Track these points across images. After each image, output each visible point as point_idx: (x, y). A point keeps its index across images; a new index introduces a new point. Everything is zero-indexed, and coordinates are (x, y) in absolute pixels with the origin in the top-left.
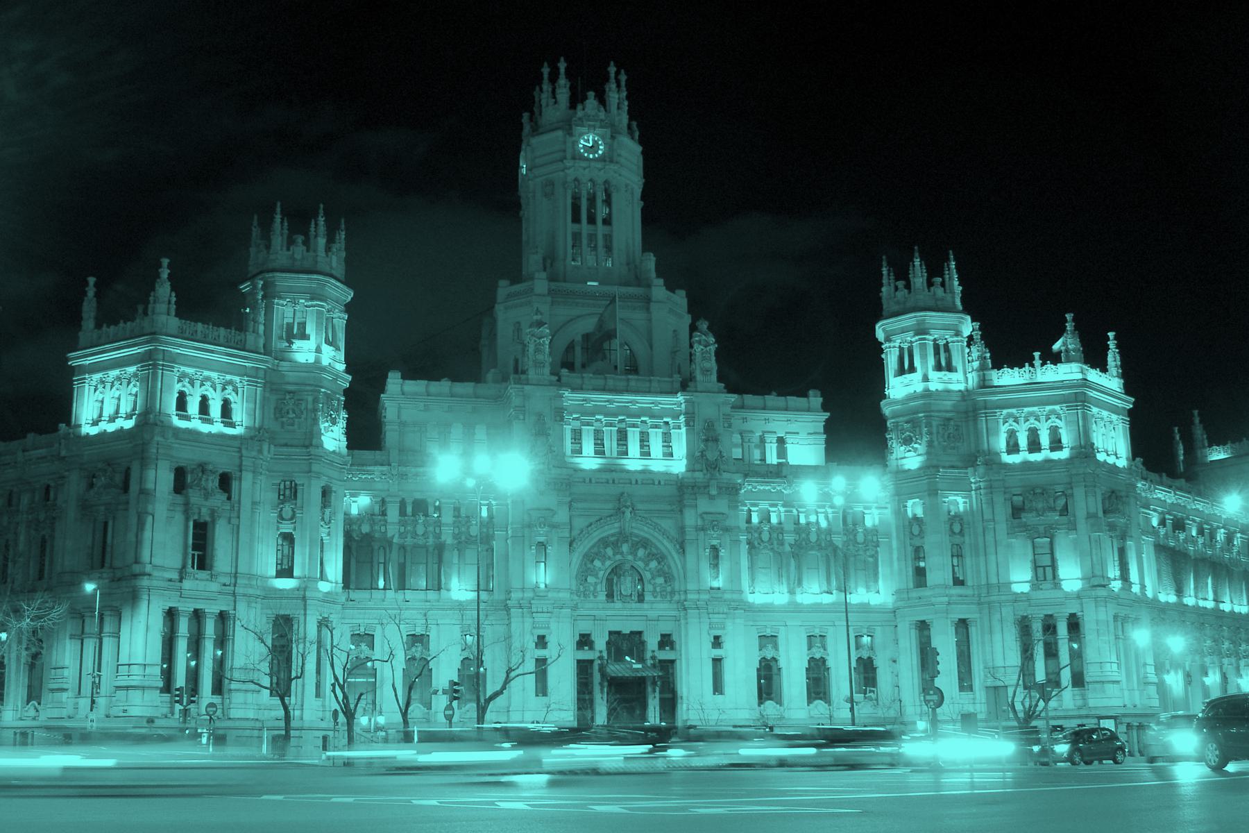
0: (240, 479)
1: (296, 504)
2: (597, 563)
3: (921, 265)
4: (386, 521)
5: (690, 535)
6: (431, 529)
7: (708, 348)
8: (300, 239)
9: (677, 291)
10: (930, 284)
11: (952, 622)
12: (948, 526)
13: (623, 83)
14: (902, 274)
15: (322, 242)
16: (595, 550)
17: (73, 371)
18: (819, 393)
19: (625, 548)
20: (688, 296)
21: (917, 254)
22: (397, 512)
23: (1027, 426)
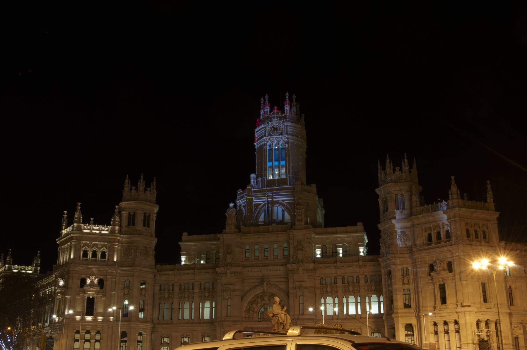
0: (106, 281)
1: (129, 289)
2: (254, 306)
3: (390, 163)
4: (174, 293)
5: (291, 291)
6: (190, 295)
7: (300, 211)
8: (133, 188)
9: (312, 185)
10: (394, 170)
11: (403, 325)
12: (401, 281)
13: (294, 99)
14: (384, 168)
15: (141, 188)
16: (253, 300)
17: (58, 245)
18: (361, 224)
19: (266, 299)
20: (317, 187)
21: (388, 158)
22: (364, 281)
23: (436, 231)
